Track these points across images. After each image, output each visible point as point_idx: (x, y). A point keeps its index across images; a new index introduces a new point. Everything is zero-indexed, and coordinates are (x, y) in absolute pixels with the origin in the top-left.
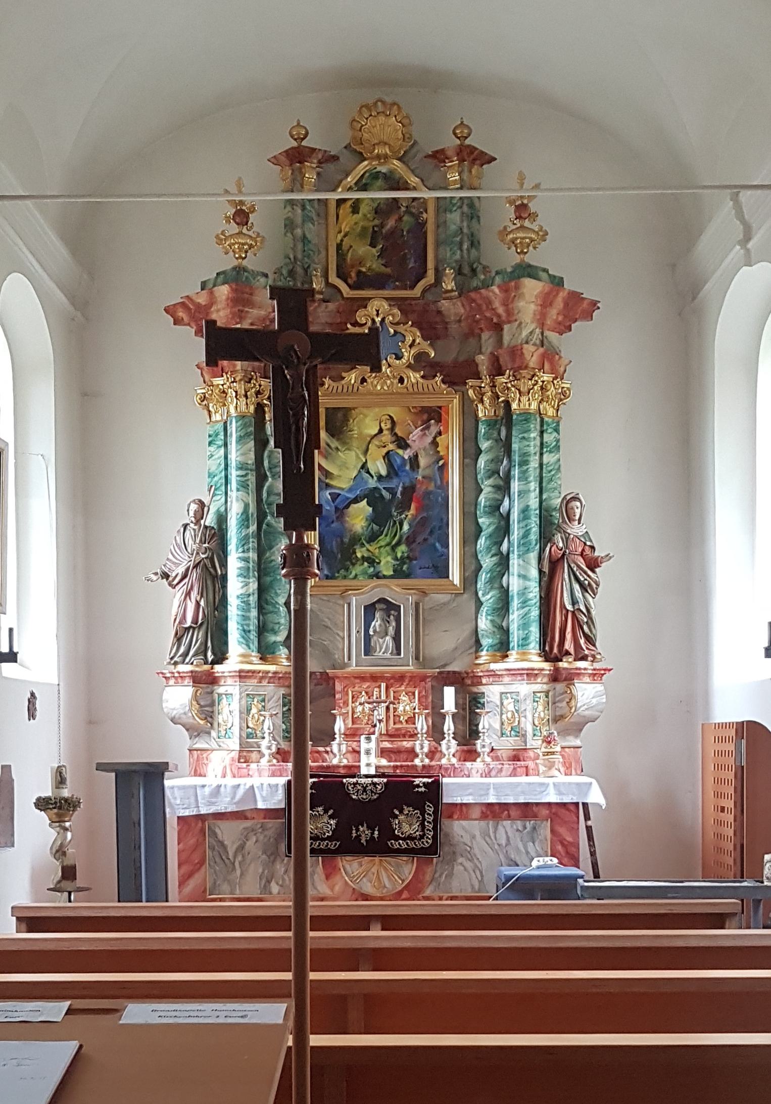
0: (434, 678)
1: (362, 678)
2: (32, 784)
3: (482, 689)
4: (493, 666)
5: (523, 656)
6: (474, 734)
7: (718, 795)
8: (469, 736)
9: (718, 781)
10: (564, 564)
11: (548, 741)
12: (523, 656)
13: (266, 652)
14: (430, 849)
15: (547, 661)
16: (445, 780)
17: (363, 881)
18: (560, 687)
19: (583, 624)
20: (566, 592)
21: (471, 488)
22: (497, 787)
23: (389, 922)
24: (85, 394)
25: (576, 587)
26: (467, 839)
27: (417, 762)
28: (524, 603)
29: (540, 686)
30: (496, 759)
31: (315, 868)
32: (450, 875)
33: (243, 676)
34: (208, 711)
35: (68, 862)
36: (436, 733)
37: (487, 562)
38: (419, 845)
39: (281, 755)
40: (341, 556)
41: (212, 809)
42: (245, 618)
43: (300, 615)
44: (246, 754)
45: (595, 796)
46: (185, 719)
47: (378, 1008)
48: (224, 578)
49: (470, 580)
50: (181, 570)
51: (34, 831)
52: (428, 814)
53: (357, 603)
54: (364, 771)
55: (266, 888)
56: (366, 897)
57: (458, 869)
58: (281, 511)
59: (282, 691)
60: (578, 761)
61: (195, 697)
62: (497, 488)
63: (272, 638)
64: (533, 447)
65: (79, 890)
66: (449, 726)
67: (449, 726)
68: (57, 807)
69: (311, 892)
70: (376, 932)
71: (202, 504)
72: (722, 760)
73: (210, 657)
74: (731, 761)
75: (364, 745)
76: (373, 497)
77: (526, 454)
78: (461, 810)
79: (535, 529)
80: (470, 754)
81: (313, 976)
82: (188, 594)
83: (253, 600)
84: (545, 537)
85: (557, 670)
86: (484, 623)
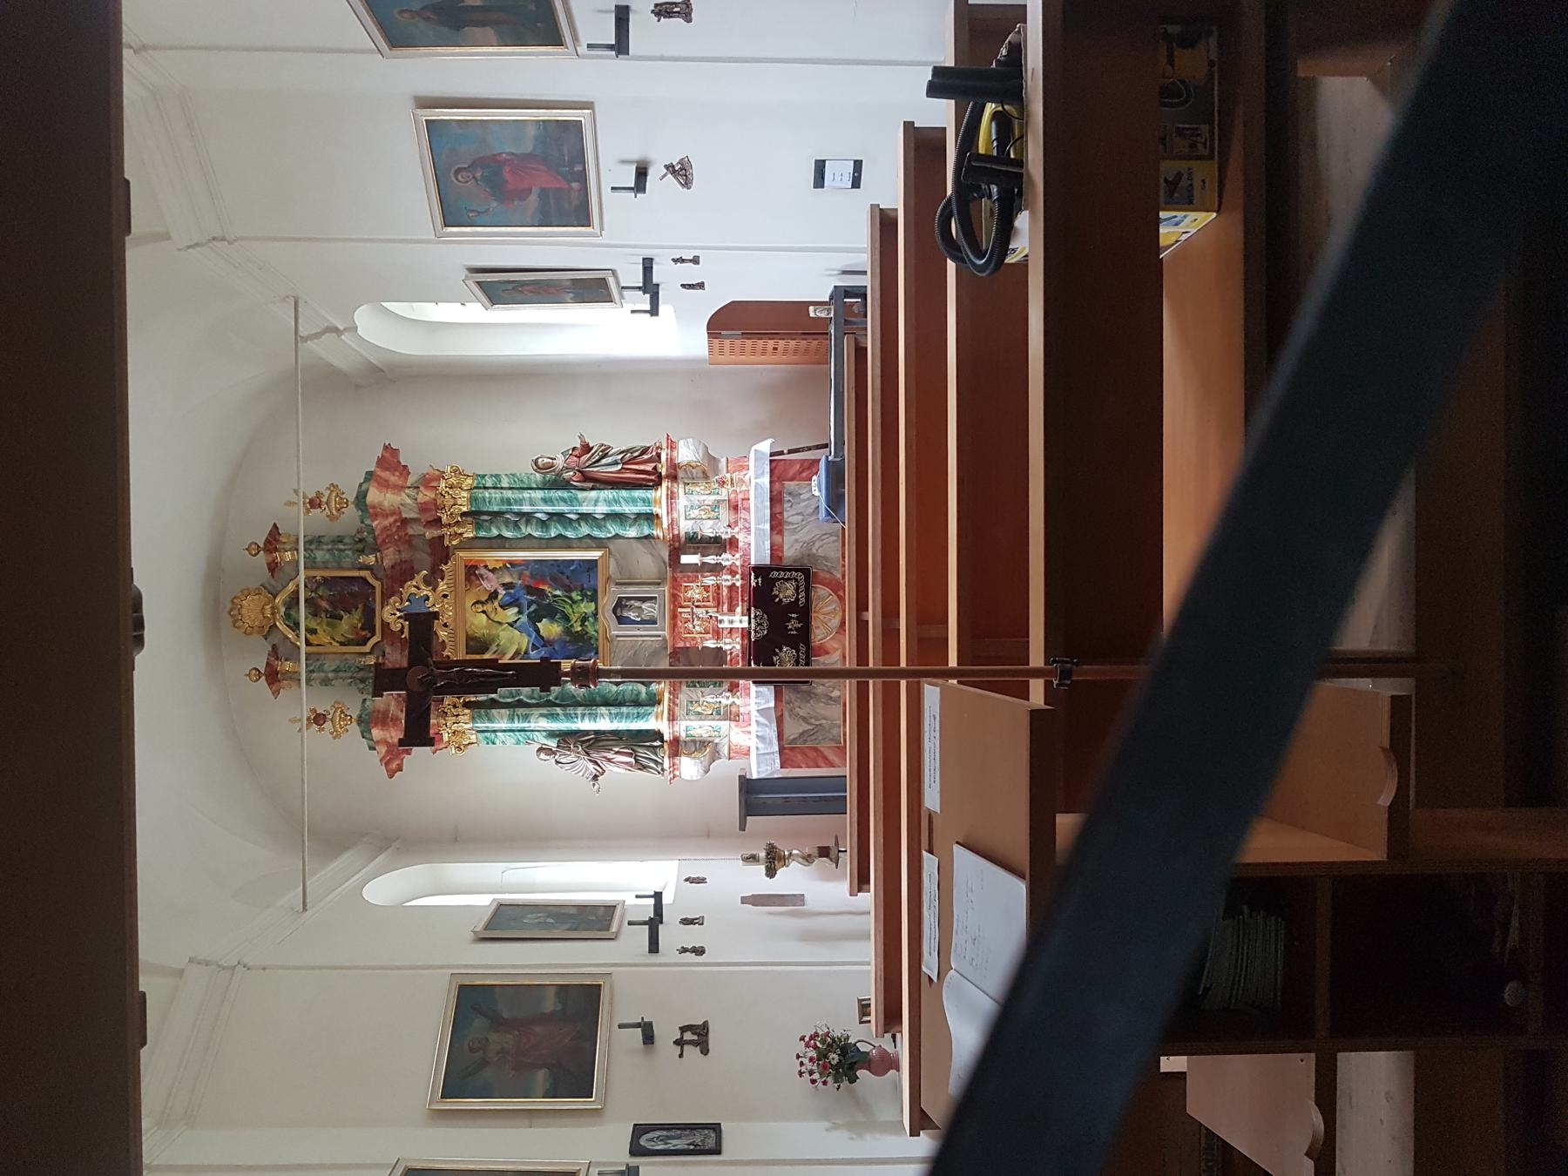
0: (674, 571)
1: (674, 626)
2: (755, 879)
3: (682, 534)
4: (665, 525)
5: (658, 502)
6: (716, 540)
7: (764, 352)
8: (718, 544)
9: (753, 352)
10: (585, 470)
11: (722, 483)
12: (658, 502)
13: (654, 701)
14: (806, 574)
15: (660, 484)
16: (753, 562)
17: (830, 624)
18: (681, 474)
19: (632, 457)
20: (607, 470)
21: (528, 542)
22: (758, 523)
23: (862, 606)
24: (456, 840)
25: (604, 461)
26: (798, 546)
27: (738, 584)
28: (617, 501)
29: (680, 490)
30: (736, 523)
31: (820, 662)
32: (826, 558)
33: (672, 718)
34: (699, 745)
35: (816, 853)
36: (716, 569)
37: (585, 530)
38: (802, 582)
39: (733, 689)
40: (580, 643)
41: (775, 742)
42: (628, 716)
43: (626, 674)
44: (733, 716)
45: (765, 447)
46: (706, 763)
47: (928, 615)
48: (597, 732)
49: (599, 543)
50: (591, 766)
51: (792, 878)
52: (419, 626)
53: (616, 631)
54: (745, 625)
55: (836, 700)
56: (843, 623)
57: (821, 552)
58: (545, 689)
59: (684, 688)
60: (738, 460)
61: (689, 755)
62: (528, 522)
63: (644, 695)
64: (497, 494)
65: (837, 844)
66: (711, 560)
67: (711, 560)
68: (774, 861)
69: (839, 666)
70: (870, 616)
71: (540, 750)
72: (737, 350)
73: (658, 743)
74: (738, 342)
75: (726, 625)
76: (535, 618)
77: (502, 500)
78: (776, 550)
79: (560, 493)
80: (732, 544)
81: (903, 664)
82: (609, 760)
83: (614, 710)
84: (566, 485)
85: (667, 477)
86: (632, 532)
